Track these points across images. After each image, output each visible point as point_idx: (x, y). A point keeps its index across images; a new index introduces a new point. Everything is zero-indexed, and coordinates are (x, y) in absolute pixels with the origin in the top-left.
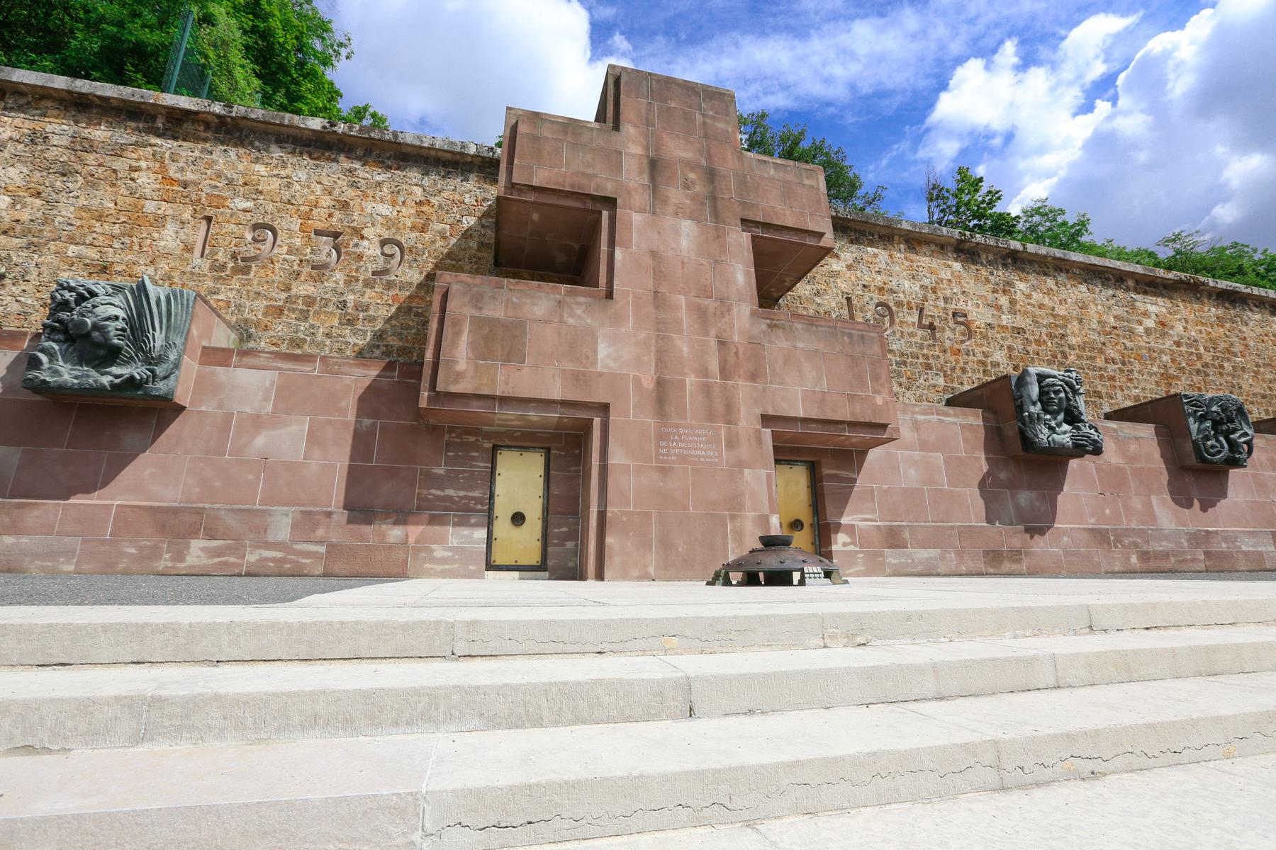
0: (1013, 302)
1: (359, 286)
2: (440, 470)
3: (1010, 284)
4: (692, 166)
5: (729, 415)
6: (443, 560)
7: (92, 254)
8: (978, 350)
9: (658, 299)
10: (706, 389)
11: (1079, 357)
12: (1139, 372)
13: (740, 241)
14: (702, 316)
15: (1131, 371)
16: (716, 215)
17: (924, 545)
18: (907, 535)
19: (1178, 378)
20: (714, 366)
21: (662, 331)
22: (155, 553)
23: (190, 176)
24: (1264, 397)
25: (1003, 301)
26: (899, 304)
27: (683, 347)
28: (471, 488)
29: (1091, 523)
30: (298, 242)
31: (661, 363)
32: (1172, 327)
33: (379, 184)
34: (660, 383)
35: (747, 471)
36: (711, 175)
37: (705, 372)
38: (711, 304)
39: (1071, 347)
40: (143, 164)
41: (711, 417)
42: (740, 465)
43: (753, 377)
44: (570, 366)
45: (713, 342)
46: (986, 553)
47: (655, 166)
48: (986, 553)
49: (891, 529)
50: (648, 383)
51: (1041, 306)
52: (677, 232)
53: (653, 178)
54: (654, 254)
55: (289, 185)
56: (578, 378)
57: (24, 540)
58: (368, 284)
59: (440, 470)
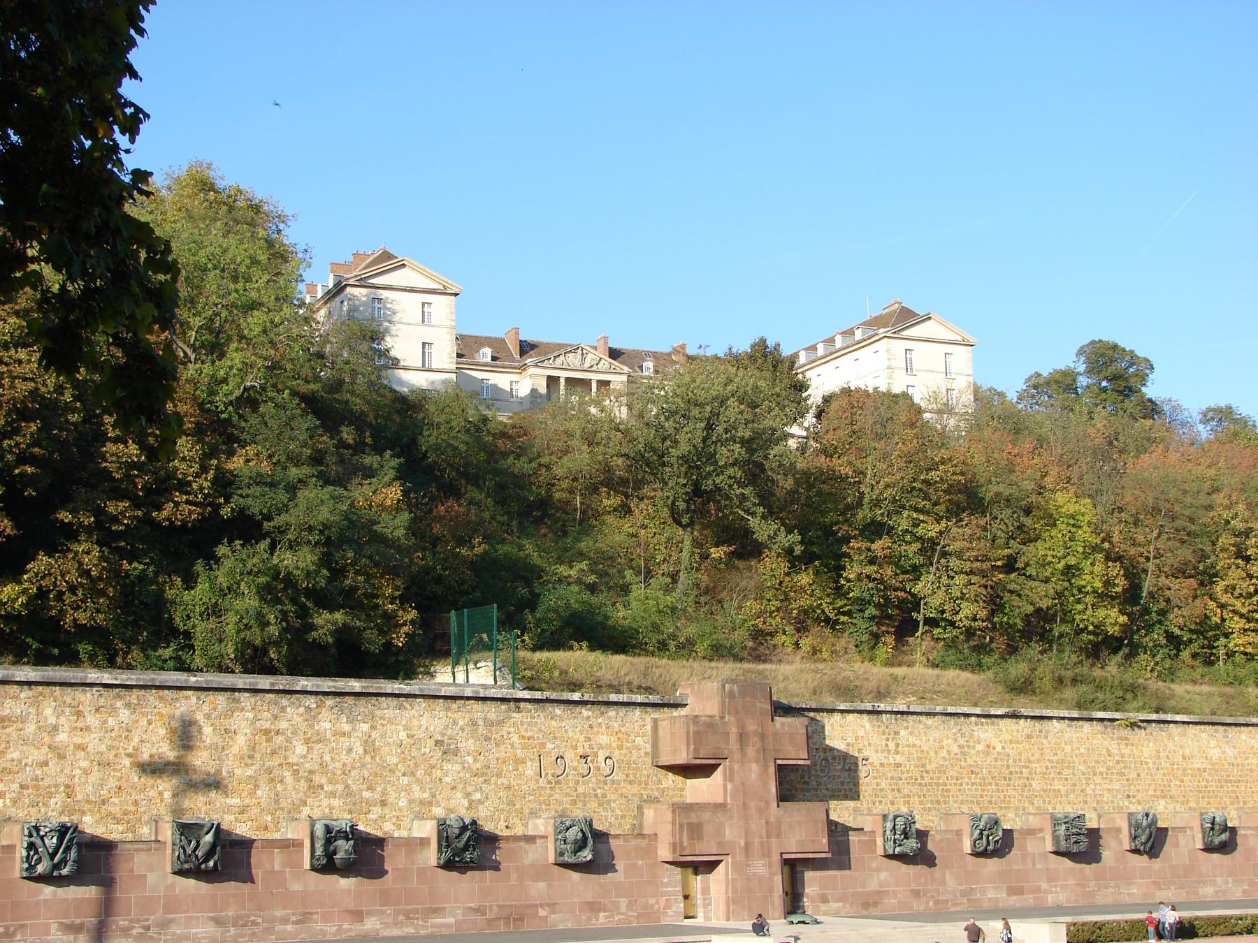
0: (897, 745)
1: (602, 785)
2: (665, 880)
3: (897, 733)
4: (755, 733)
5: (769, 855)
6: (672, 916)
7: (505, 781)
8: (874, 781)
9: (745, 806)
10: (761, 844)
11: (932, 778)
12: (967, 784)
13: (772, 770)
14: (760, 811)
15: (961, 784)
16: (765, 759)
17: (837, 901)
18: (830, 897)
19: (991, 784)
20: (764, 834)
21: (746, 818)
22: (590, 919)
23: (530, 734)
24: (1045, 791)
25: (892, 745)
26: (834, 758)
27: (753, 826)
28: (676, 887)
29: (913, 886)
30: (575, 764)
31: (747, 834)
32: (994, 748)
33: (600, 724)
34: (746, 843)
35: (775, 878)
36: (762, 737)
37: (761, 837)
38: (762, 804)
39: (927, 772)
40: (512, 729)
41: (763, 856)
42: (773, 874)
43: (778, 836)
44: (718, 840)
45: (763, 821)
46: (863, 904)
47: (743, 738)
48: (863, 904)
49: (824, 894)
50: (742, 843)
51: (914, 745)
52: (751, 770)
53: (741, 745)
54: (743, 784)
55: (566, 731)
56: (720, 844)
57: (557, 916)
58: (606, 783)
59: (665, 880)
